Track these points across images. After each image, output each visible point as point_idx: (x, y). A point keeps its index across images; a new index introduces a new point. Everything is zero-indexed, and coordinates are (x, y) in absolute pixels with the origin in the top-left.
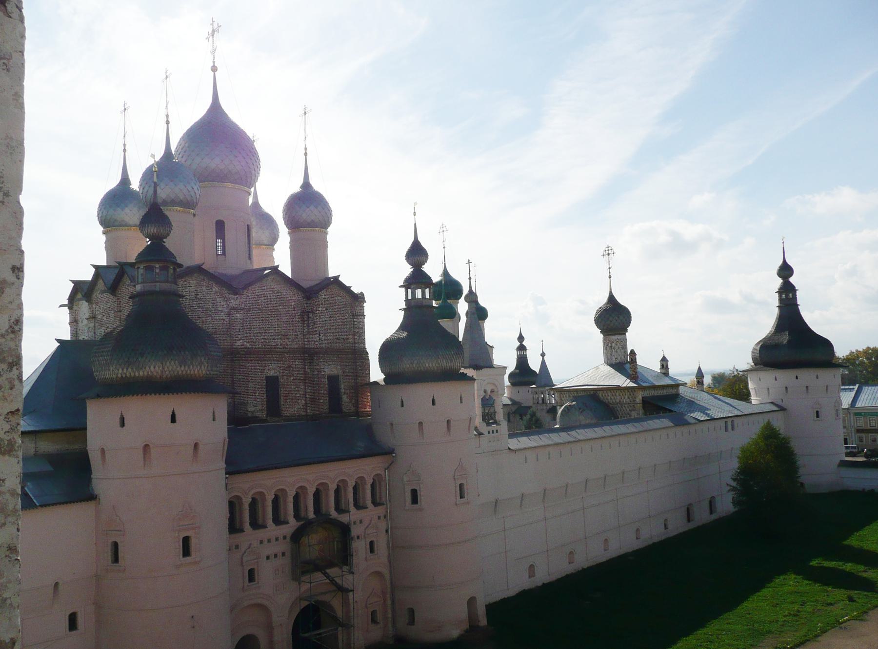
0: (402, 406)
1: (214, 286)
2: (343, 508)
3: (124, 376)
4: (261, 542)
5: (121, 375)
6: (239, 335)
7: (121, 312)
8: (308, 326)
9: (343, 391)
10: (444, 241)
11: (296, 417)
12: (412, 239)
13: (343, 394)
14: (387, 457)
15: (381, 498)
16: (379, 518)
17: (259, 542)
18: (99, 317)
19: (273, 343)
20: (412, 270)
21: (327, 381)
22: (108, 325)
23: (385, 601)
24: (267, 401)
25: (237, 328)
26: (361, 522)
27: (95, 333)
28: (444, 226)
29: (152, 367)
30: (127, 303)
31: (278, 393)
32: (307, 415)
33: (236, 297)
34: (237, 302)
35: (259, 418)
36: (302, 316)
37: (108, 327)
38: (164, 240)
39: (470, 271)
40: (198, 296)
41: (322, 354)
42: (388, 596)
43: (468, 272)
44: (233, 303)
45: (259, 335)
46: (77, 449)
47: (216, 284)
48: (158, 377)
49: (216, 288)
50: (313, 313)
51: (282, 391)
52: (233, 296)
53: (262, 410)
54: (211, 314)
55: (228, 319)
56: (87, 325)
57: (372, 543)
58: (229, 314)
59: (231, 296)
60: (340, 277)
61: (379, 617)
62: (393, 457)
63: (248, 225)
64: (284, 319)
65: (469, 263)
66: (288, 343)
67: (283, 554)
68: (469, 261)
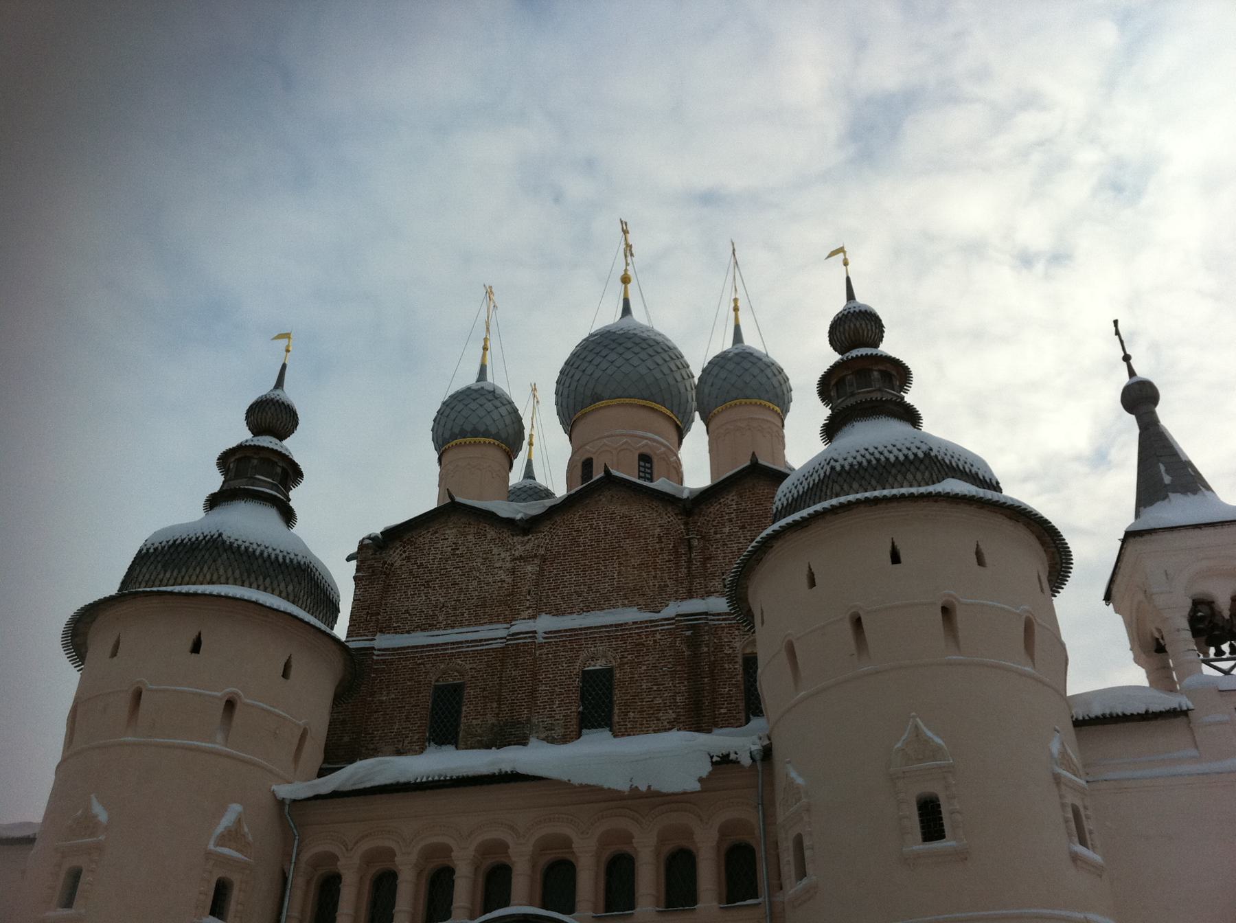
25: (525, 589)
34: (528, 547)
40: (458, 552)
44: (519, 551)
49: (491, 533)
51: (617, 695)
52: (520, 538)
58: (513, 571)
59: (515, 539)
64: (636, 561)
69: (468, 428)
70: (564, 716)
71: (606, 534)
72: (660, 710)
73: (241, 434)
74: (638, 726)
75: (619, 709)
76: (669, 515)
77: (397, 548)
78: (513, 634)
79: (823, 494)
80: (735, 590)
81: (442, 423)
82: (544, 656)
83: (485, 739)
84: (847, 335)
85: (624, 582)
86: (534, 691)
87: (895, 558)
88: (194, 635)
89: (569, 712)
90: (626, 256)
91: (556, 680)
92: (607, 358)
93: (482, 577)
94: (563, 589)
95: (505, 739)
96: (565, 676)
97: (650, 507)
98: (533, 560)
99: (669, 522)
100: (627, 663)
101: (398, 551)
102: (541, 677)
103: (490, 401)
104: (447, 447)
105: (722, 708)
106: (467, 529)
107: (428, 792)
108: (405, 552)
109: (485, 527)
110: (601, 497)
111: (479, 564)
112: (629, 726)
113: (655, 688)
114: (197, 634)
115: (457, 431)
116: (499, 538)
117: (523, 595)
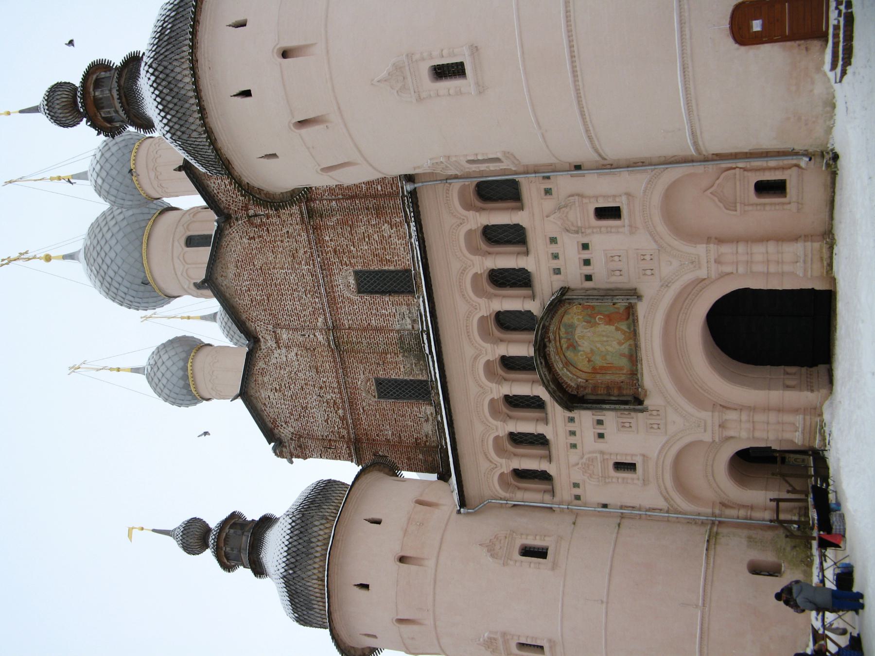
4: (574, 446)
6: (309, 336)
16: (548, 192)
17: (573, 450)
25: (301, 339)
33: (262, 340)
34: (268, 338)
40: (278, 388)
44: (271, 343)
45: (302, 301)
47: (254, 365)
49: (261, 364)
51: (375, 267)
52: (262, 344)
53: (408, 305)
58: (288, 347)
59: (263, 347)
66: (302, 251)
69: (182, 383)
70: (393, 306)
71: (252, 280)
72: (383, 235)
73: (208, 555)
74: (396, 251)
75: (385, 266)
76: (232, 232)
77: (280, 431)
78: (336, 346)
79: (201, 144)
80: (285, 202)
81: (181, 402)
82: (350, 322)
83: (414, 361)
84: (68, 115)
85: (288, 265)
86: (377, 329)
87: (247, 93)
88: (357, 589)
89: (389, 303)
90: (29, 259)
91: (367, 313)
92: (113, 277)
93: (295, 370)
95: (413, 347)
96: (363, 307)
97: (227, 247)
99: (237, 232)
100: (350, 261)
101: (282, 431)
102: (366, 324)
103: (159, 369)
104: (198, 397)
105: (377, 189)
106: (260, 382)
107: (454, 417)
108: (282, 426)
109: (257, 370)
110: (223, 284)
111: (285, 372)
112: (396, 258)
113: (367, 240)
114: (355, 587)
115: (185, 391)
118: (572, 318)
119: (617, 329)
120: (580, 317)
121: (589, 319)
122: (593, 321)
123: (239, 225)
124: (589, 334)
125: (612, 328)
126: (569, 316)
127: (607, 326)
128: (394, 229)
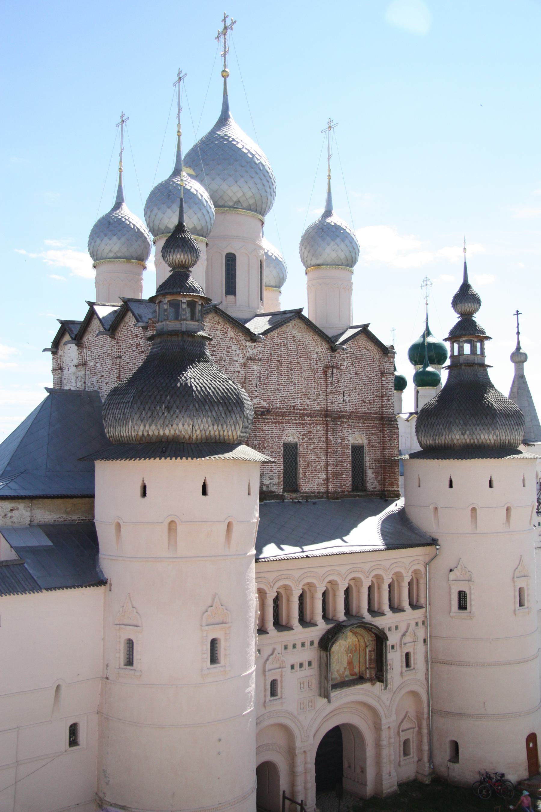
0: (451, 486)
1: (229, 331)
2: (376, 610)
3: (146, 434)
4: (286, 647)
5: (143, 431)
6: (256, 391)
7: (120, 357)
8: (331, 383)
9: (367, 464)
10: (427, 296)
11: (316, 494)
12: (461, 282)
13: (368, 468)
14: (428, 548)
15: (418, 601)
16: (417, 624)
18: (91, 364)
19: (292, 403)
20: (459, 319)
21: (350, 451)
22: (103, 374)
23: (420, 727)
24: (284, 474)
25: (254, 383)
26: (396, 628)
27: (85, 383)
28: (427, 279)
29: (180, 426)
30: (130, 348)
31: (296, 464)
32: (327, 492)
34: (255, 351)
35: (274, 494)
36: (325, 373)
37: (103, 376)
38: (190, 269)
39: (518, 324)
41: (347, 419)
42: (425, 723)
43: (516, 326)
44: (251, 353)
45: (277, 392)
46: (76, 520)
47: (232, 328)
48: (187, 437)
50: (338, 368)
51: (301, 462)
53: (278, 484)
54: (225, 364)
55: (243, 372)
56: (74, 373)
57: (407, 655)
58: (245, 366)
60: (370, 326)
61: (413, 747)
62: (437, 549)
63: (260, 261)
64: (306, 374)
65: (518, 314)
66: (309, 403)
67: (310, 664)
68: (517, 312)
72: (319, 473)
74: (310, 481)
75: (303, 470)
76: (322, 347)
82: (267, 432)
89: (280, 469)
93: (227, 366)
94: (272, 386)
96: (277, 446)
98: (258, 363)
99: (321, 352)
100: (305, 443)
102: (265, 445)
106: (216, 326)
109: (228, 328)
112: (307, 481)
113: (317, 460)
116: (236, 338)
117: (253, 387)
118: (350, 638)
119: (345, 668)
120: (351, 643)
121: (350, 649)
122: (349, 652)
123: (327, 357)
124: (342, 650)
125: (345, 665)
126: (351, 636)
127: (346, 662)
128: (323, 482)
